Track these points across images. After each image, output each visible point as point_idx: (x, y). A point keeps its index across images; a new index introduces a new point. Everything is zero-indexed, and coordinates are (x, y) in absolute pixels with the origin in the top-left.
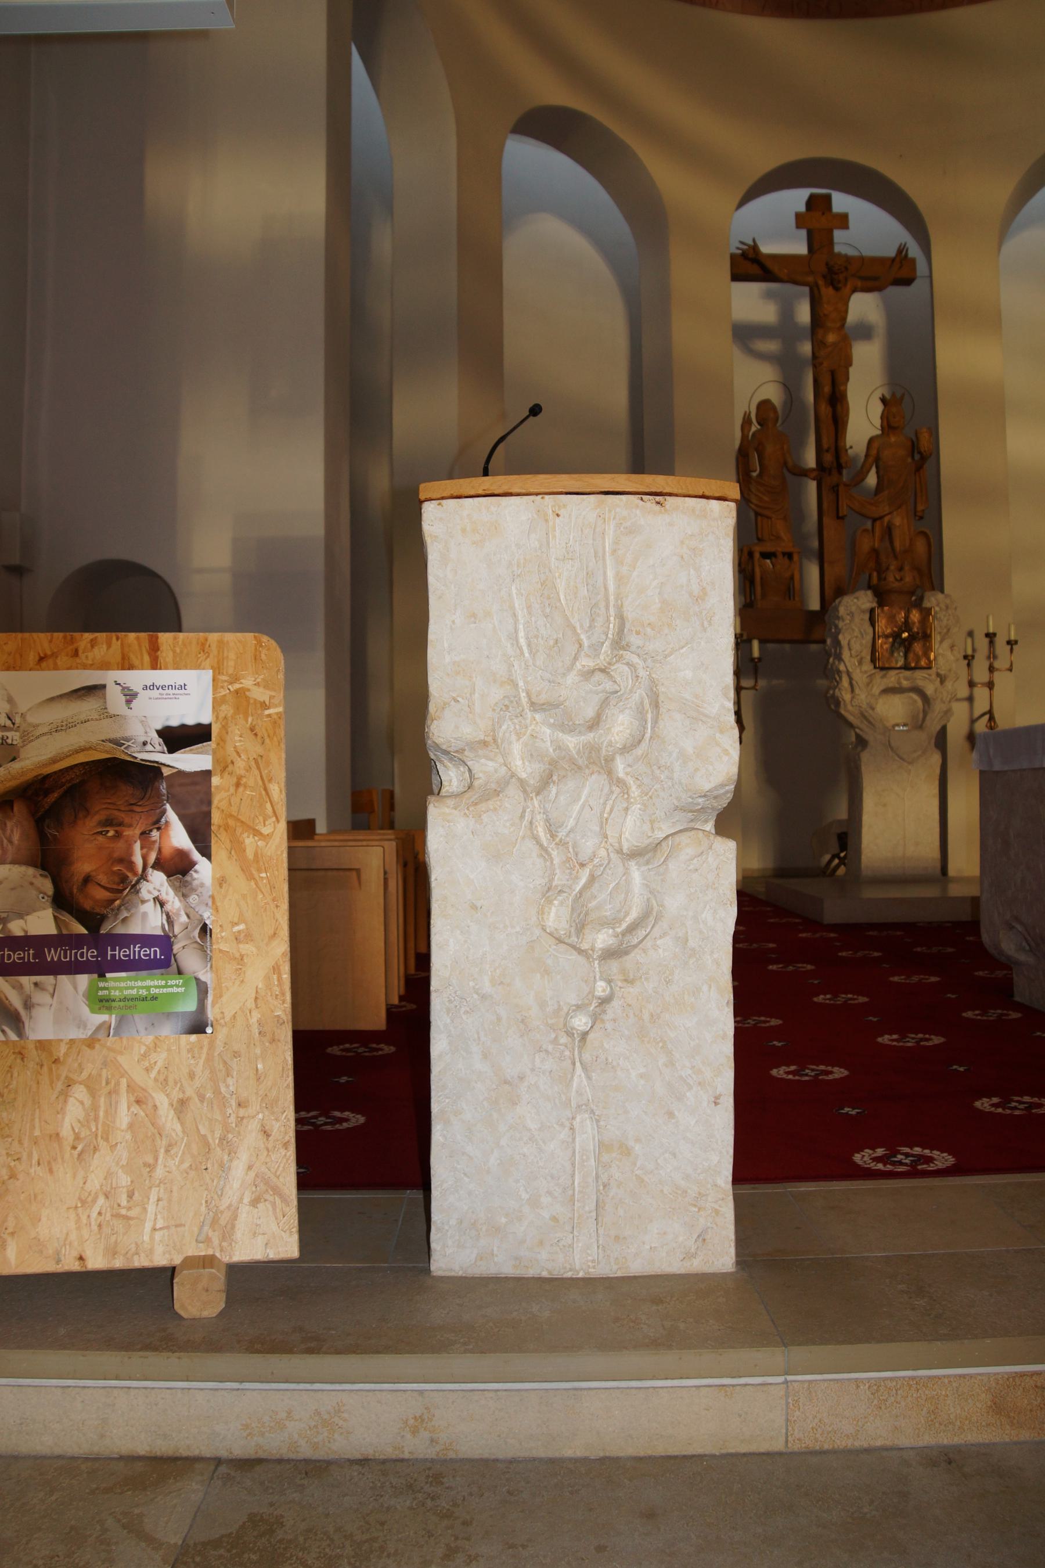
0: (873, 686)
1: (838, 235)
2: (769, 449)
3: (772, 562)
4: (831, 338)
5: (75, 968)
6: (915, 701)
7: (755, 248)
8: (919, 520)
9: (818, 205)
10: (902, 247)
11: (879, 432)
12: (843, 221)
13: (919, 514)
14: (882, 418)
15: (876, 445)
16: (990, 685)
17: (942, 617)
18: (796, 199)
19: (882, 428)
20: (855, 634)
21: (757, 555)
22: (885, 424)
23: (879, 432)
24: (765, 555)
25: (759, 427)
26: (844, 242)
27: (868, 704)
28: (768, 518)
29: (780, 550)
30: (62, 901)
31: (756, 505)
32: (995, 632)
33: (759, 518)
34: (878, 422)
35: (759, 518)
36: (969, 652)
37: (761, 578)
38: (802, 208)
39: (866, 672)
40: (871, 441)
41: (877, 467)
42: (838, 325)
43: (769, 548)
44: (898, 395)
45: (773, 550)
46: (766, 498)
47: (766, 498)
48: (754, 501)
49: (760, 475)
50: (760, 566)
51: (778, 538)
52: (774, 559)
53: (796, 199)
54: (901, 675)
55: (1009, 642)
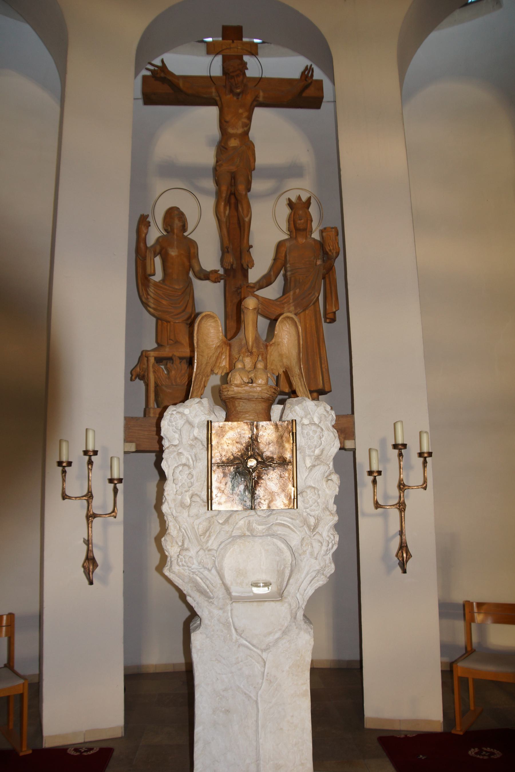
0: (209, 536)
2: (173, 253)
3: (166, 369)
4: (233, 143)
6: (280, 550)
8: (330, 322)
10: (309, 67)
13: (331, 316)
14: (289, 221)
15: (283, 250)
17: (311, 433)
20: (184, 461)
22: (292, 226)
23: (286, 237)
24: (159, 360)
25: (165, 233)
27: (199, 563)
28: (168, 322)
29: (177, 354)
31: (154, 309)
32: (405, 443)
33: (160, 322)
34: (284, 226)
35: (160, 322)
36: (375, 468)
37: (157, 386)
39: (197, 516)
40: (280, 245)
41: (286, 271)
42: (240, 131)
43: (166, 352)
44: (304, 199)
45: (170, 355)
46: (164, 302)
47: (164, 302)
48: (152, 305)
50: (154, 372)
51: (177, 342)
52: (169, 365)
54: (251, 519)
55: (421, 455)
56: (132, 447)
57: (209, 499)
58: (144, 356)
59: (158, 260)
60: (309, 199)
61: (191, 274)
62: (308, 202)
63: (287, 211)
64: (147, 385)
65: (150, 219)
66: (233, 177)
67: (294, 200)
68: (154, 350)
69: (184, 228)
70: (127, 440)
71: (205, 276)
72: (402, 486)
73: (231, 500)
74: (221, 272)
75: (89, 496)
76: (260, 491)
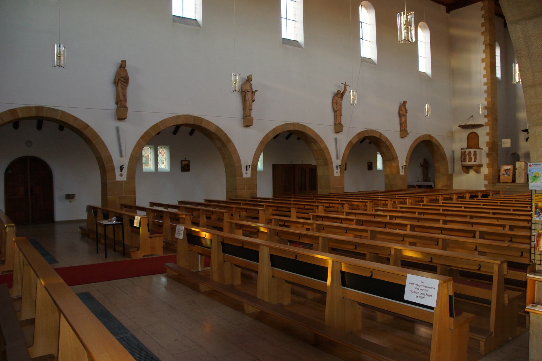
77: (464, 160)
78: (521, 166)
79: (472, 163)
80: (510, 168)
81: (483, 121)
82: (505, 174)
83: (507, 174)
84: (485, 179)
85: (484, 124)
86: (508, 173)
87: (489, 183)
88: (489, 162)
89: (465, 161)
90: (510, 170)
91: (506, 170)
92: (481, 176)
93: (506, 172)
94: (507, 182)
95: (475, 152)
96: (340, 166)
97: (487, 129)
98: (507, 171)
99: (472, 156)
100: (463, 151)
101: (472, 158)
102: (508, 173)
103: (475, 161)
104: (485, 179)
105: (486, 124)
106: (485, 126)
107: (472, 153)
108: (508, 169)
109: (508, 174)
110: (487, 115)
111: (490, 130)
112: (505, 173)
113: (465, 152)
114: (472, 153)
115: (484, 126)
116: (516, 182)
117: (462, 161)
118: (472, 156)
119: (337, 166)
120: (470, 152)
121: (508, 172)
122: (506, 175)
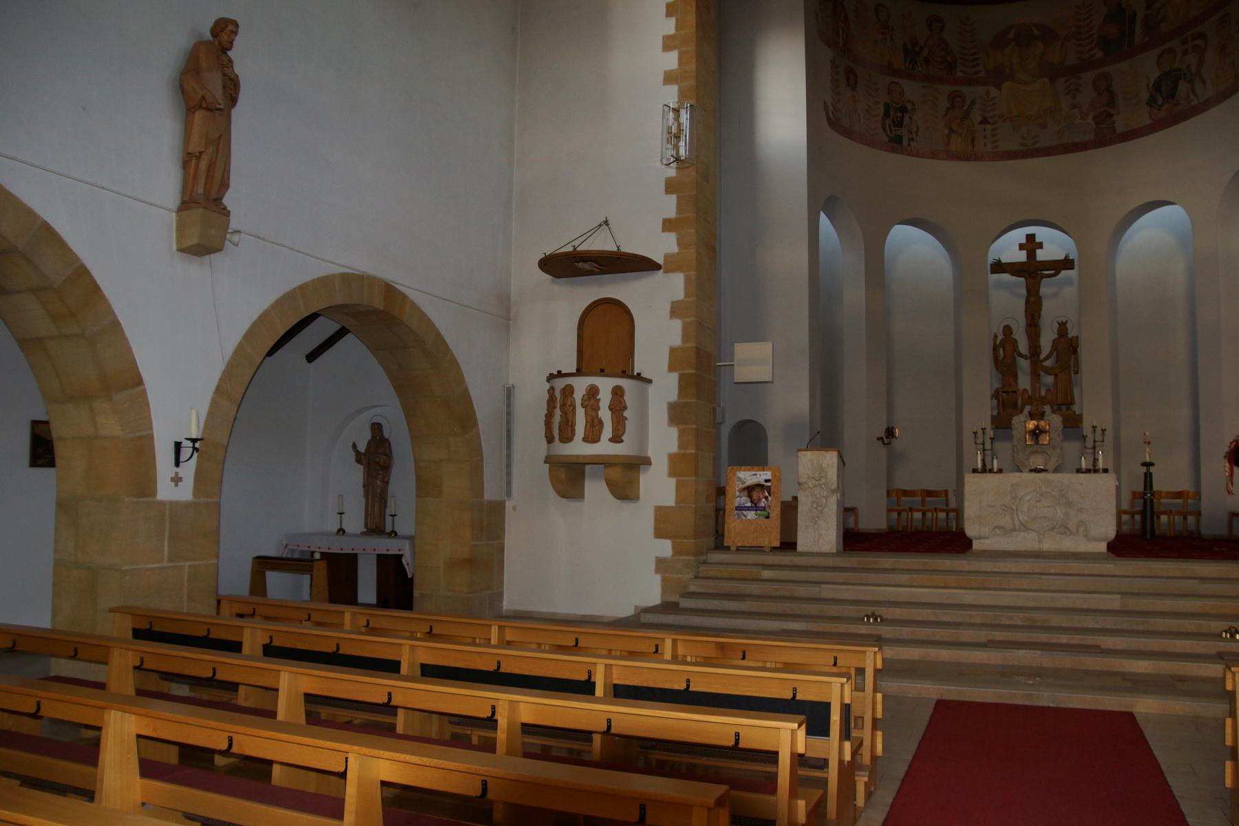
1: (1038, 252)
5: (753, 510)
7: (999, 261)
9: (1031, 238)
11: (1057, 336)
12: (1040, 245)
16: (1094, 448)
18: (1019, 235)
19: (1058, 334)
21: (1000, 393)
23: (1057, 336)
24: (1003, 392)
26: (1041, 255)
30: (752, 502)
37: (1002, 401)
38: (1024, 241)
40: (1054, 341)
43: (1006, 389)
49: (1003, 359)
51: (1010, 385)
53: (1019, 235)
56: (994, 427)
57: (1026, 441)
58: (997, 391)
59: (1001, 350)
60: (1067, 322)
61: (1015, 354)
62: (1067, 322)
63: (1057, 326)
64: (998, 401)
65: (998, 334)
66: (1033, 315)
67: (1060, 322)
68: (1001, 388)
69: (1012, 334)
70: (992, 424)
71: (1021, 355)
72: (1095, 441)
73: (1031, 441)
74: (1029, 355)
75: (983, 444)
76: (1040, 439)
77: (560, 431)
78: (822, 469)
79: (604, 447)
80: (767, 481)
81: (659, 246)
82: (748, 509)
83: (755, 507)
84: (660, 533)
85: (660, 261)
86: (763, 503)
87: (677, 551)
88: (680, 447)
89: (567, 437)
90: (769, 489)
91: (750, 490)
92: (641, 516)
93: (750, 496)
94: (758, 549)
95: (618, 392)
96: (194, 441)
97: (674, 286)
98: (755, 495)
99: (605, 414)
100: (560, 383)
101: (601, 423)
102: (763, 503)
103: (616, 439)
104: (660, 533)
105: (672, 264)
106: (666, 272)
107: (605, 398)
108: (759, 486)
109: (764, 509)
110: (676, 219)
111: (687, 294)
112: (749, 504)
113: (568, 391)
114: (605, 398)
115: (661, 271)
116: (800, 548)
117: (550, 439)
118: (605, 414)
119: (178, 446)
120: (593, 392)
121: (760, 500)
122: (751, 515)
